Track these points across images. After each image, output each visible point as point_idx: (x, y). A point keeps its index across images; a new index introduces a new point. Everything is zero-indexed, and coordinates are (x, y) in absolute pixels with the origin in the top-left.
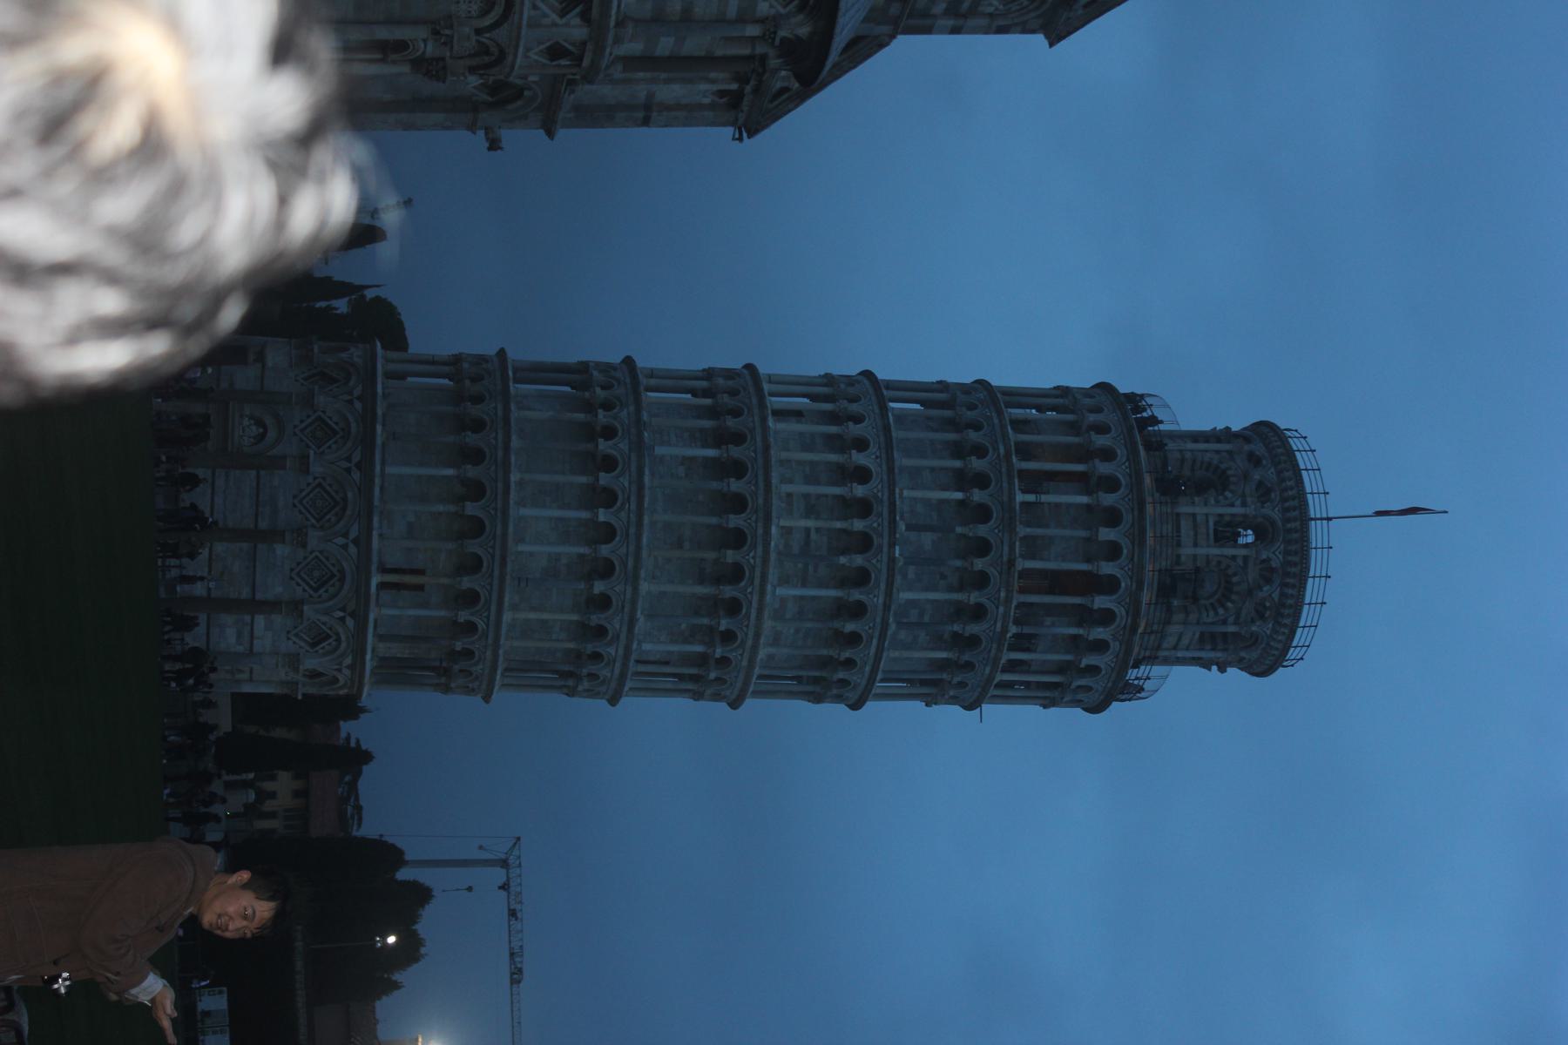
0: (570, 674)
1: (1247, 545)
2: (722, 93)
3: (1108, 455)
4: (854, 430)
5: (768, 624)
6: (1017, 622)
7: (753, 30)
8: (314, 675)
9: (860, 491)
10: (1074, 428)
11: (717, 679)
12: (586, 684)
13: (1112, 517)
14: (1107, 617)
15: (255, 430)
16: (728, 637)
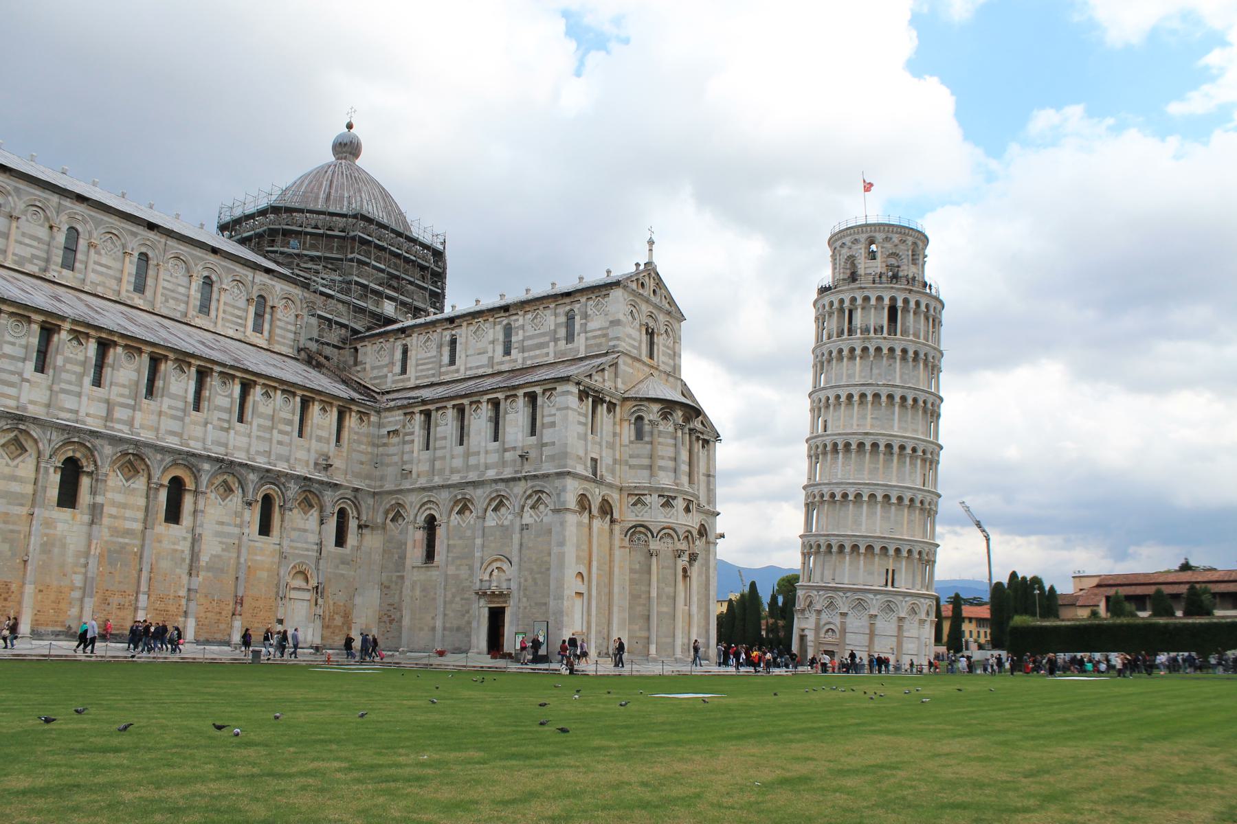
0: (929, 512)
1: (877, 247)
2: (703, 447)
3: (842, 301)
4: (832, 400)
6: (908, 336)
7: (679, 433)
8: (928, 614)
9: (856, 398)
10: (830, 314)
11: (931, 454)
12: (933, 507)
13: (866, 299)
14: (906, 301)
15: (830, 633)
16: (914, 450)
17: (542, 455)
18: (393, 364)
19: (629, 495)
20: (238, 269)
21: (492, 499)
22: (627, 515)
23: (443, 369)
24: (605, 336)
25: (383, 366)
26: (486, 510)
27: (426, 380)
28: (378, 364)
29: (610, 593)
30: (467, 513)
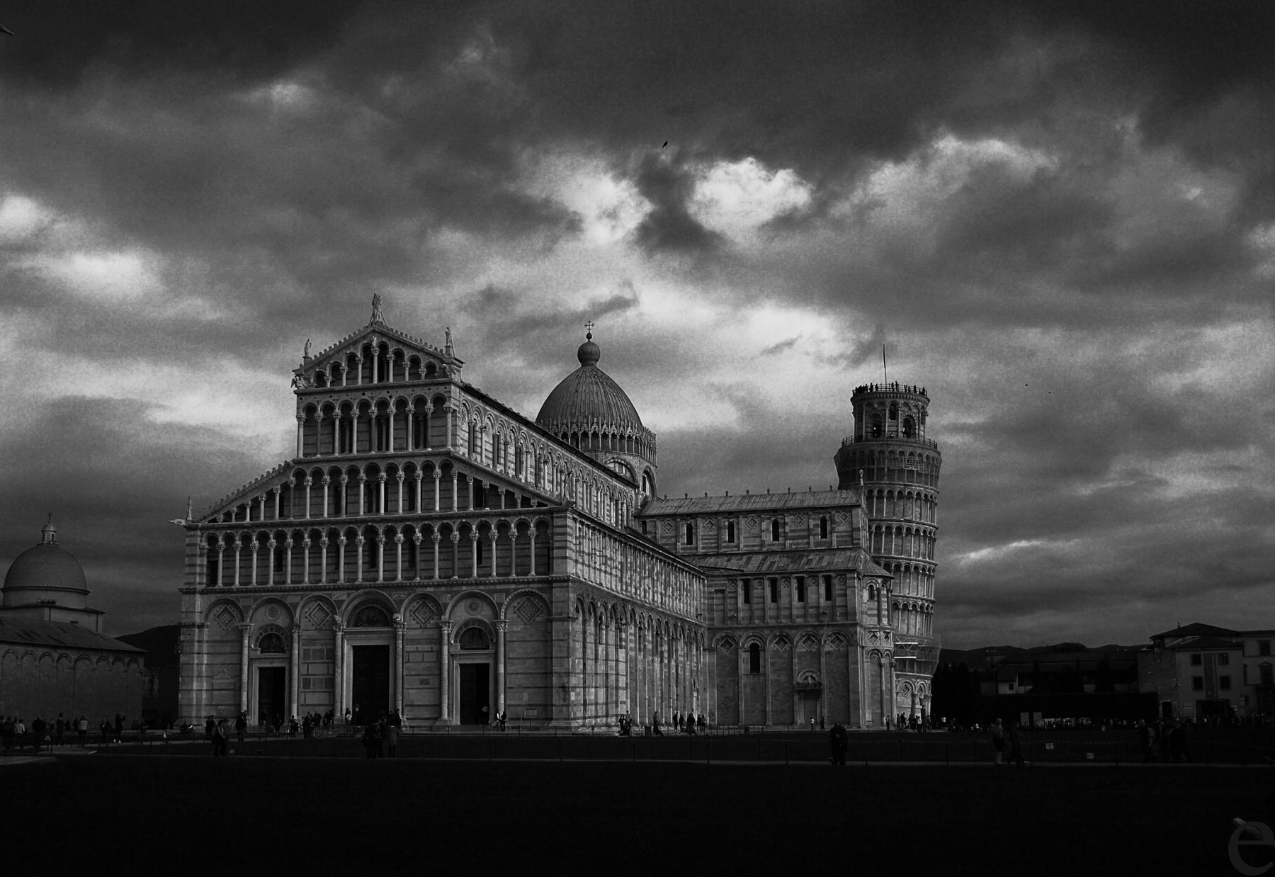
3: (872, 452)
5: (921, 558)
16: (923, 569)
17: (836, 612)
18: (677, 537)
19: (869, 632)
20: (609, 480)
21: (804, 636)
22: (870, 645)
23: (725, 544)
24: (849, 536)
25: (671, 537)
26: (798, 642)
27: (710, 550)
28: (667, 535)
29: (864, 688)
30: (782, 643)
